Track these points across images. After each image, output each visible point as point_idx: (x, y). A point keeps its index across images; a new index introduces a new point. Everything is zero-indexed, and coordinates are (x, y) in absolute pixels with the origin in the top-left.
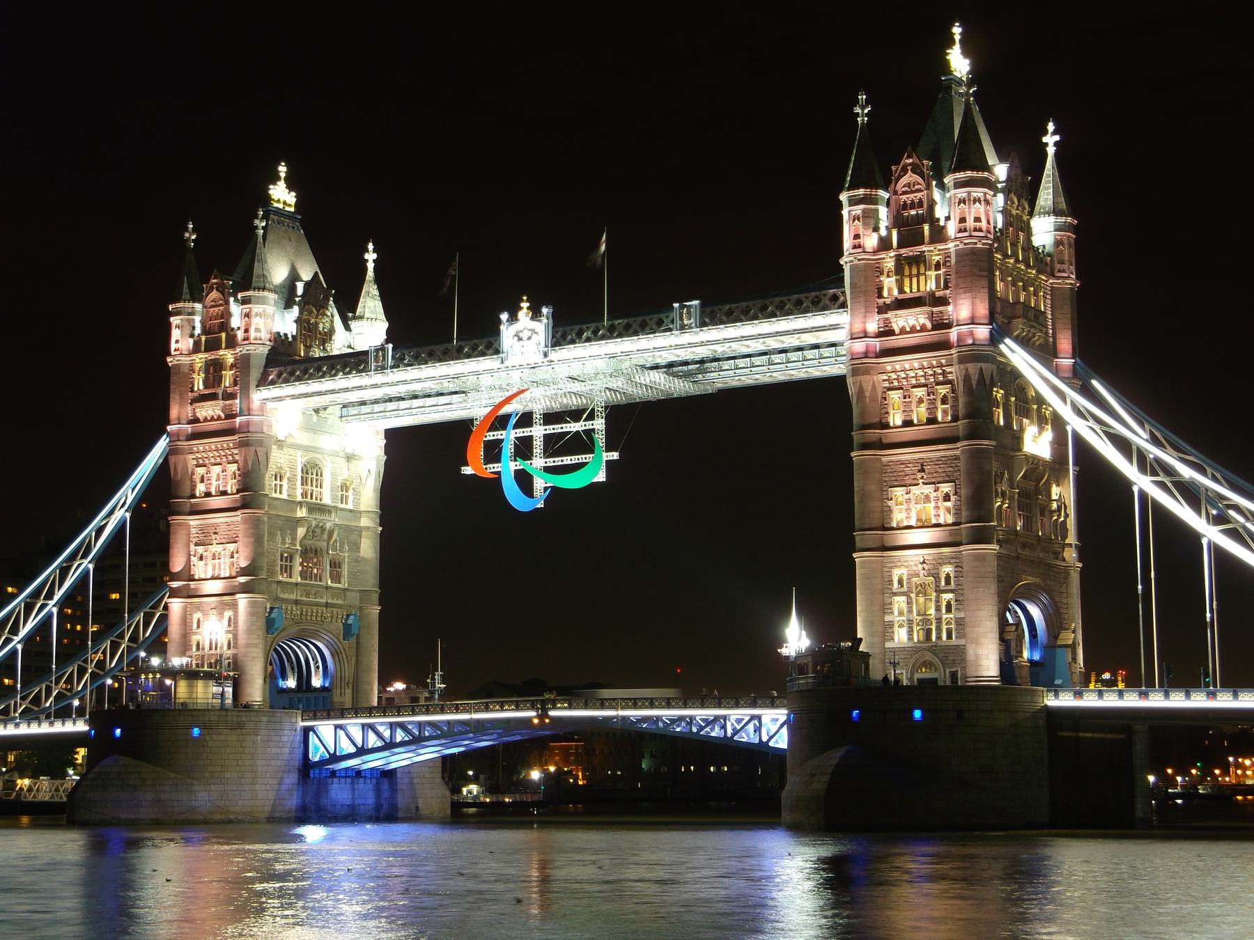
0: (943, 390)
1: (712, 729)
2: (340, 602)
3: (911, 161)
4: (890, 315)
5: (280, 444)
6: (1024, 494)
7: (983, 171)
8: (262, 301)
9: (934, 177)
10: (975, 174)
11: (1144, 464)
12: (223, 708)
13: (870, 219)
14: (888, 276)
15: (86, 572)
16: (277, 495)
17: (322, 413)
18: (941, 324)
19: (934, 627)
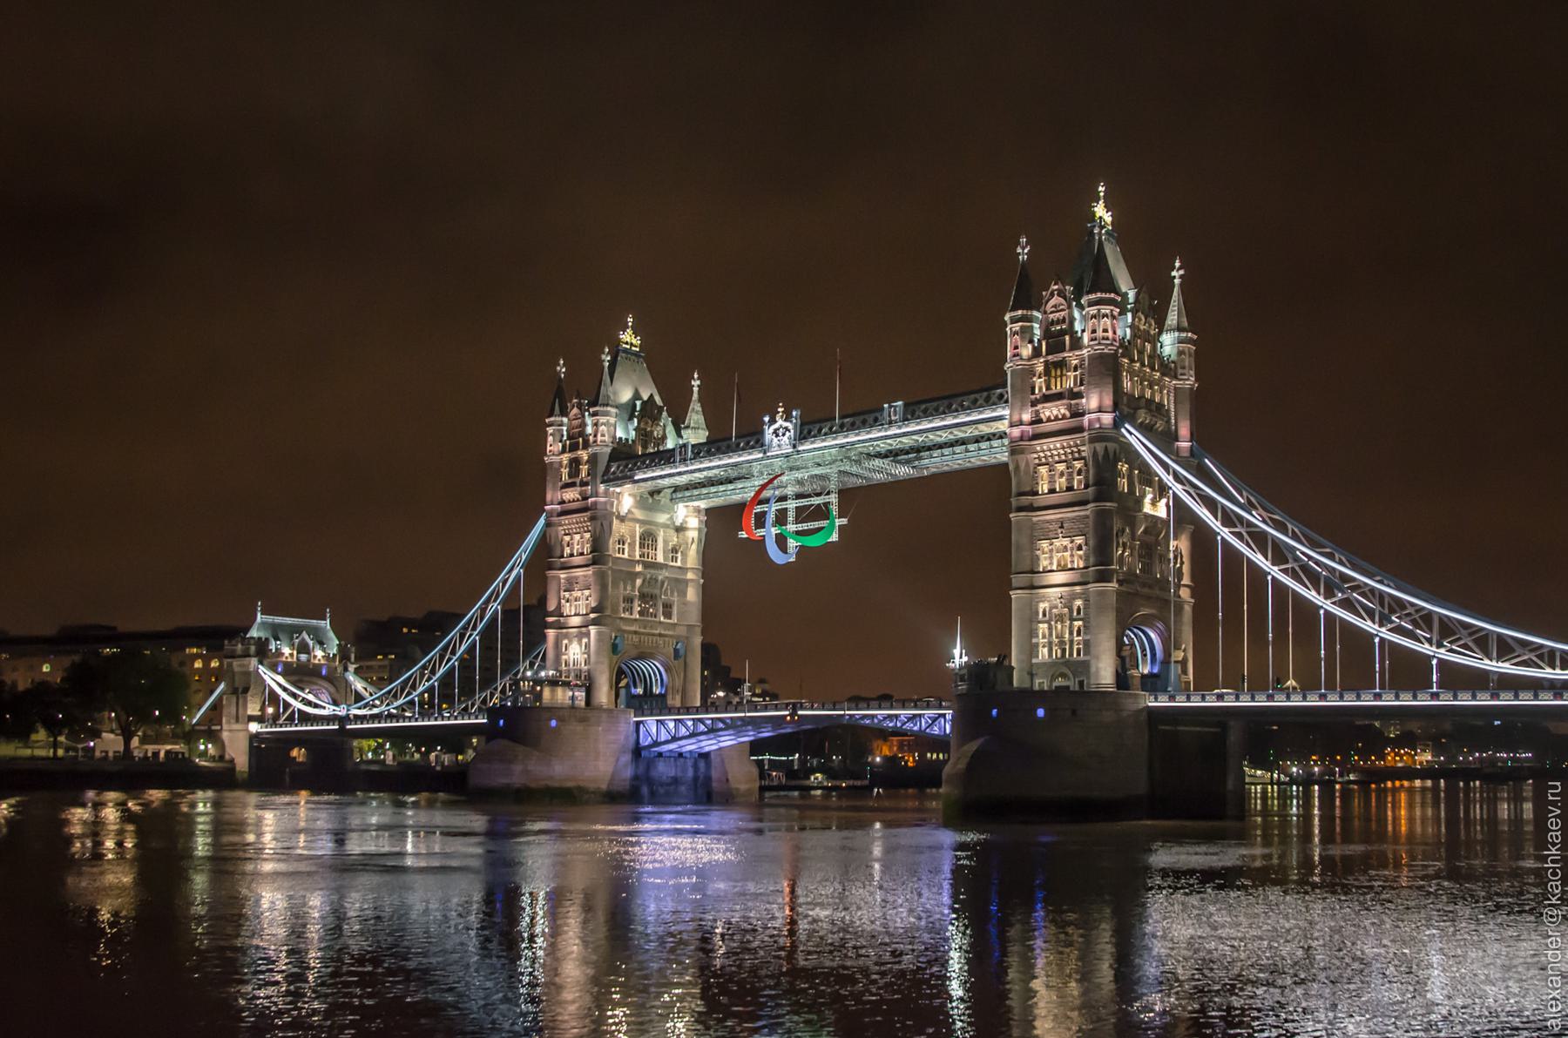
0: (1078, 465)
2: (670, 633)
3: (1056, 287)
5: (622, 519)
7: (1110, 293)
8: (606, 414)
9: (1074, 299)
10: (1104, 295)
11: (1228, 519)
12: (573, 707)
13: (1026, 334)
14: (1040, 377)
15: (496, 610)
16: (621, 555)
17: (656, 497)
18: (1077, 413)
19: (1067, 647)
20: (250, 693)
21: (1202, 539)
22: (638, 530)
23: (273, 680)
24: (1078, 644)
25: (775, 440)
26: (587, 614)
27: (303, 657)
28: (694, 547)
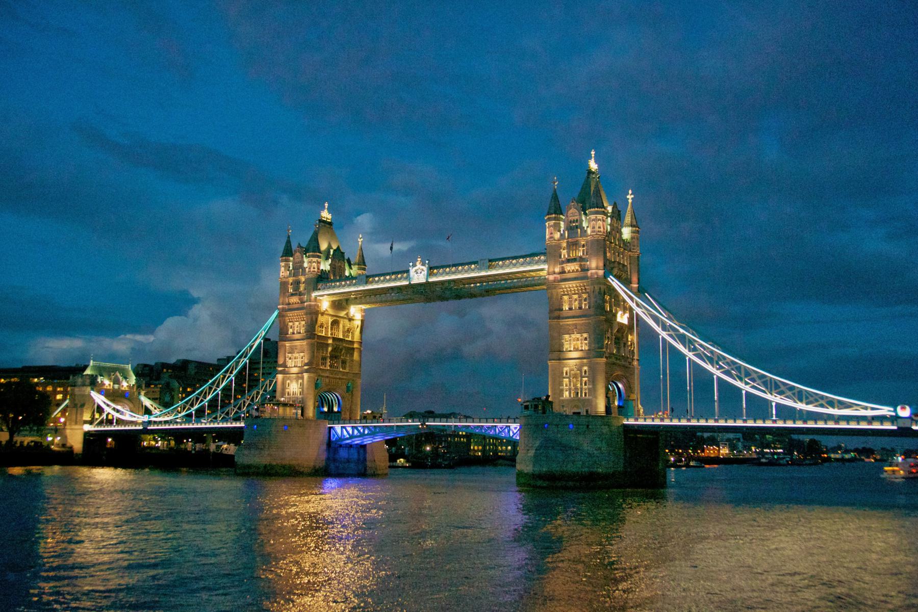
0: (585, 296)
1: (491, 431)
2: (345, 377)
4: (564, 265)
5: (323, 314)
6: (617, 339)
10: (599, 209)
11: (664, 328)
15: (246, 363)
18: (584, 269)
19: (579, 391)
20: (85, 407)
21: (648, 336)
22: (330, 320)
23: (99, 399)
24: (585, 390)
25: (416, 275)
26: (302, 367)
27: (116, 386)
28: (359, 329)
